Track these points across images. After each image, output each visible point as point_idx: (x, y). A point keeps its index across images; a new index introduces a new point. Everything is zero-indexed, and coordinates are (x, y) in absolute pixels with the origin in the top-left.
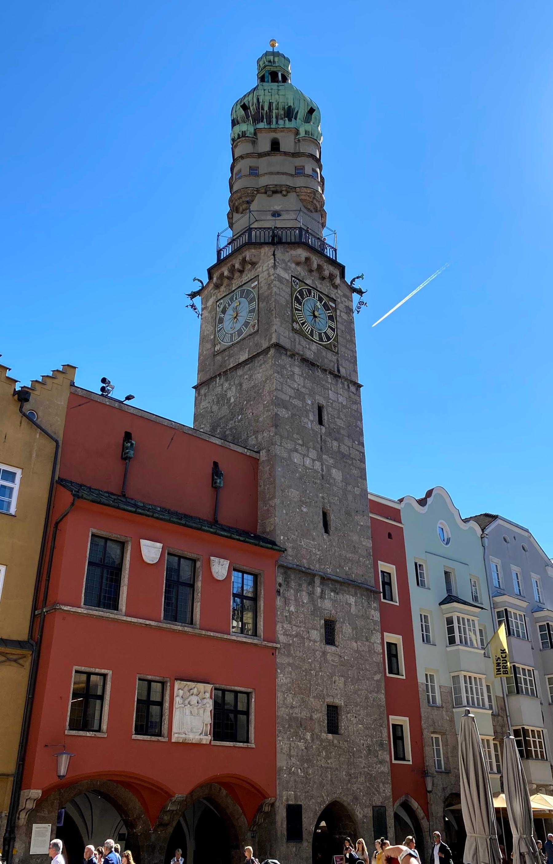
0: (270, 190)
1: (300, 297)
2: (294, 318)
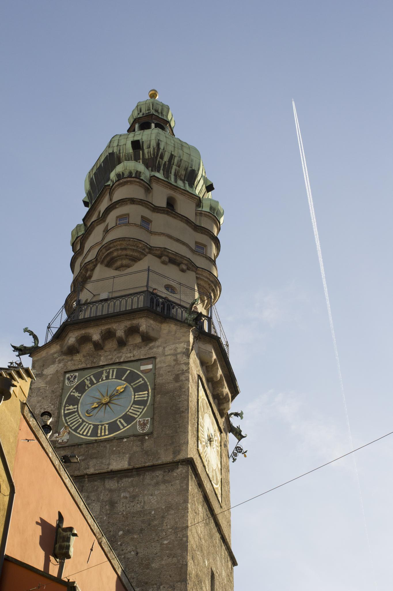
0: (167, 256)
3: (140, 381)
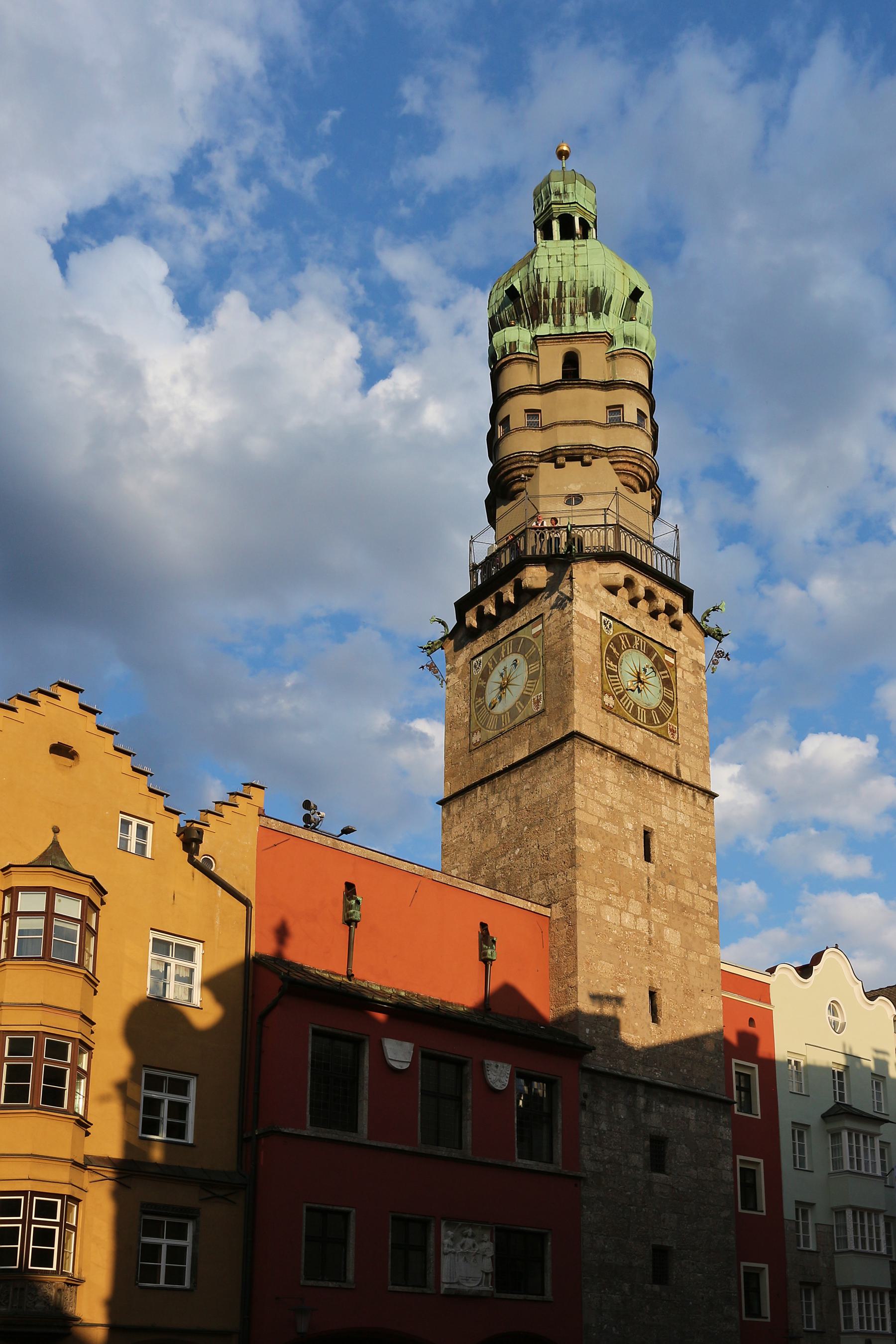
1: (615, 650)
2: (605, 687)
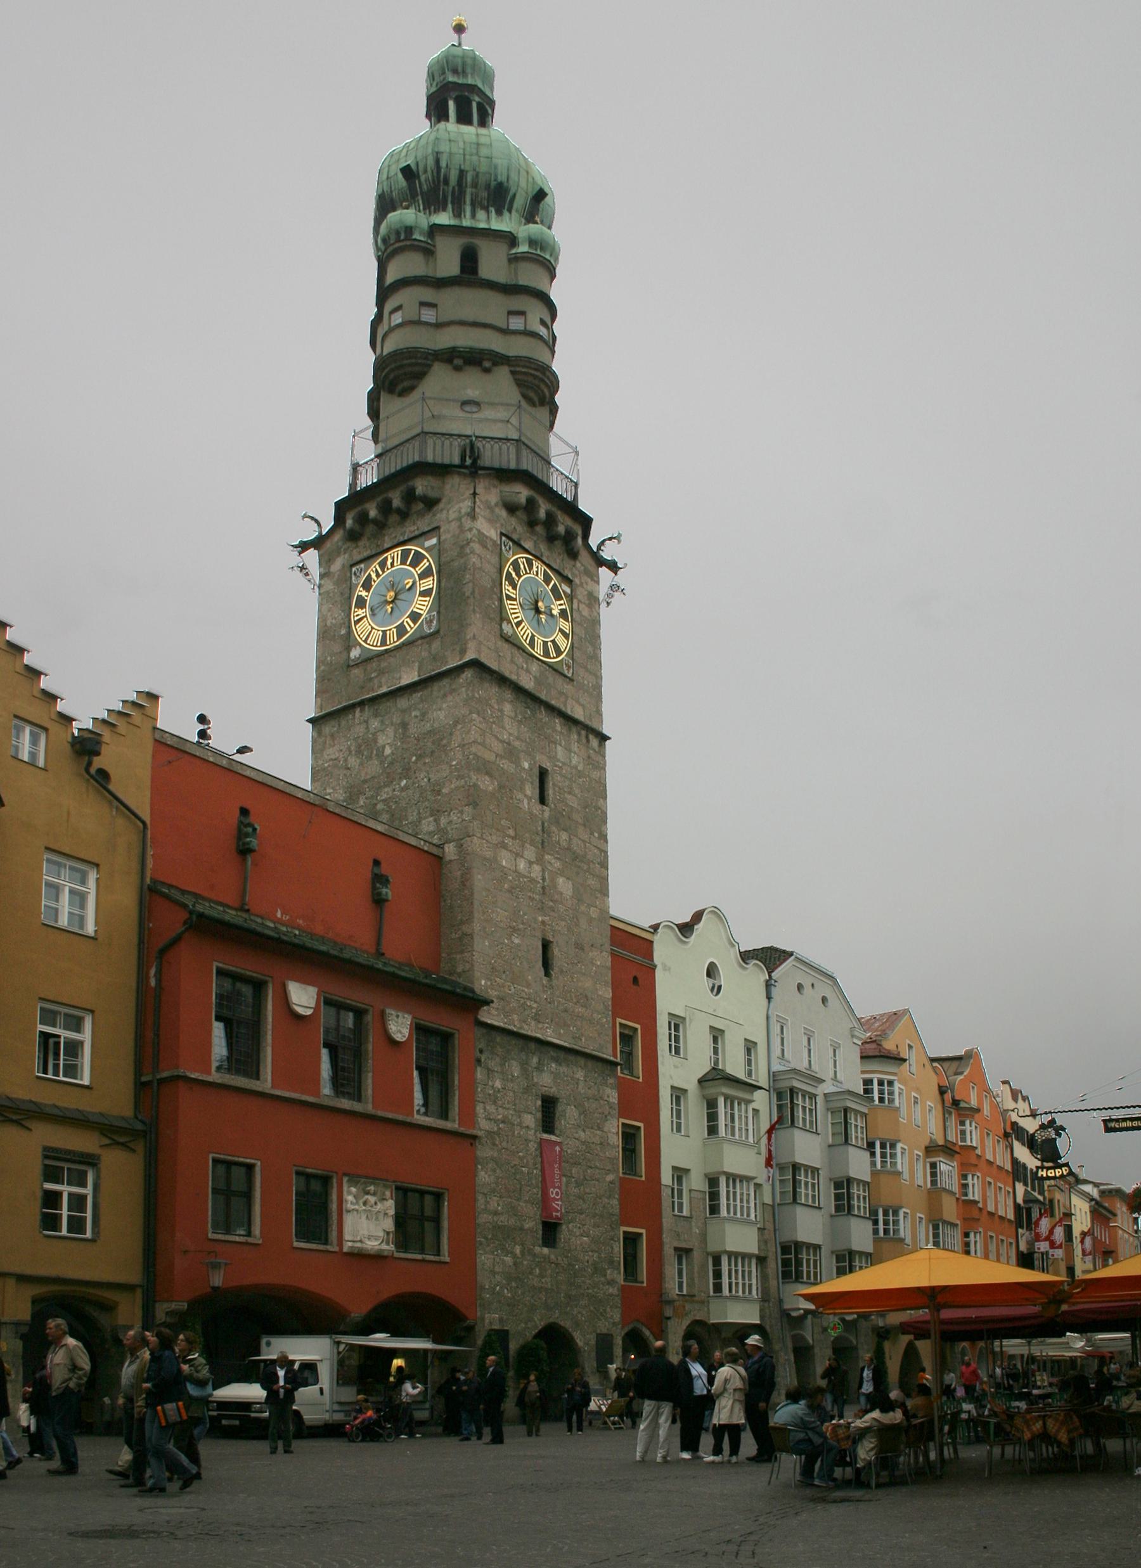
3: (424, 564)
